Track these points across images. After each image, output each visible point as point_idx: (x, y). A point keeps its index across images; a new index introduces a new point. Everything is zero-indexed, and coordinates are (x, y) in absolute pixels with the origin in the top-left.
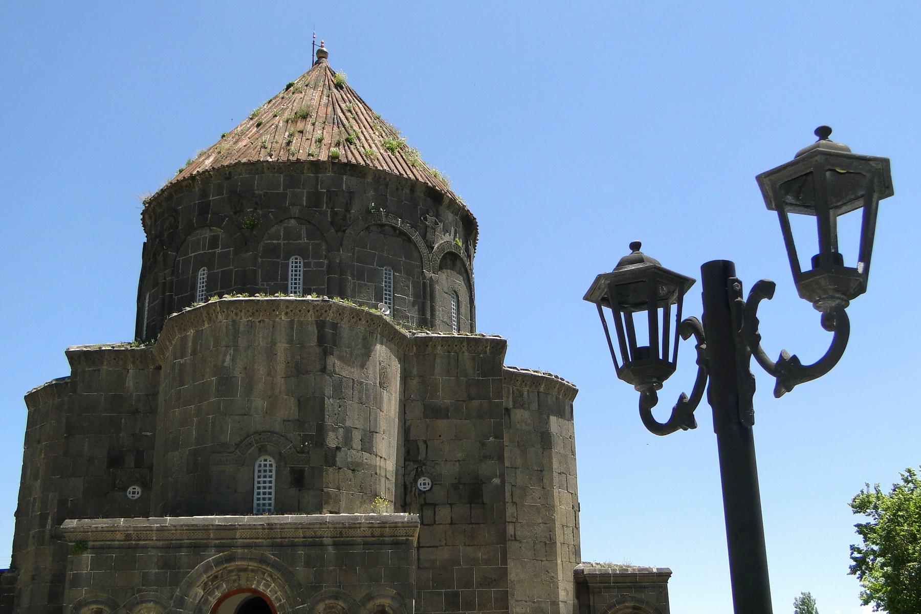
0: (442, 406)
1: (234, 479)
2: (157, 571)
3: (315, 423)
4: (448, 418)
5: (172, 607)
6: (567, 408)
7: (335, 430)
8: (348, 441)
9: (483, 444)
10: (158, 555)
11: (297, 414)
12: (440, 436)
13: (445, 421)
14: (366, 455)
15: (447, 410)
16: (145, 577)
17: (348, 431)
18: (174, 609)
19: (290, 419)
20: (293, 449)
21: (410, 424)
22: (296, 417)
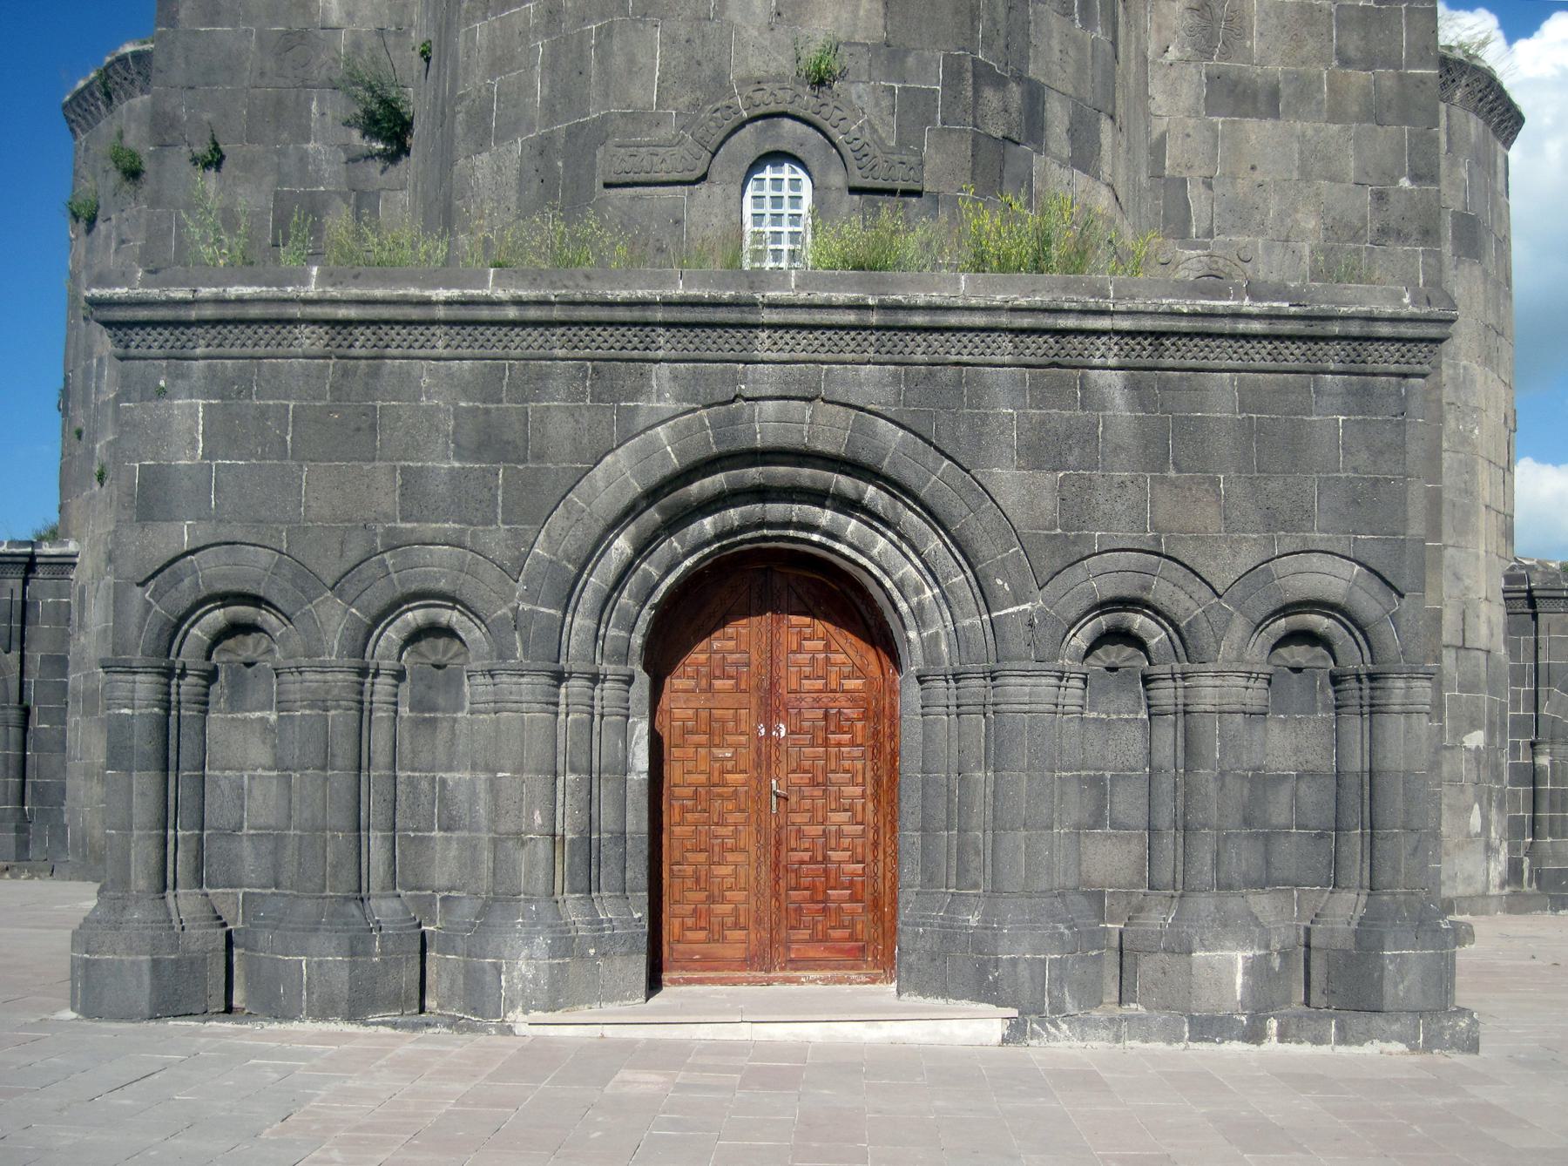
0: (1259, 80)
1: (678, 222)
2: (457, 465)
3: (940, 56)
4: (1276, 116)
5: (522, 598)
6: (1500, 161)
7: (1000, 83)
8: (1034, 126)
9: (1380, 197)
10: (456, 407)
11: (881, 22)
12: (1253, 168)
13: (1268, 124)
14: (1081, 179)
15: (1274, 94)
16: (412, 483)
17: (1035, 95)
18: (524, 606)
19: (858, 38)
20: (867, 131)
21: (1164, 128)
22: (880, 34)
